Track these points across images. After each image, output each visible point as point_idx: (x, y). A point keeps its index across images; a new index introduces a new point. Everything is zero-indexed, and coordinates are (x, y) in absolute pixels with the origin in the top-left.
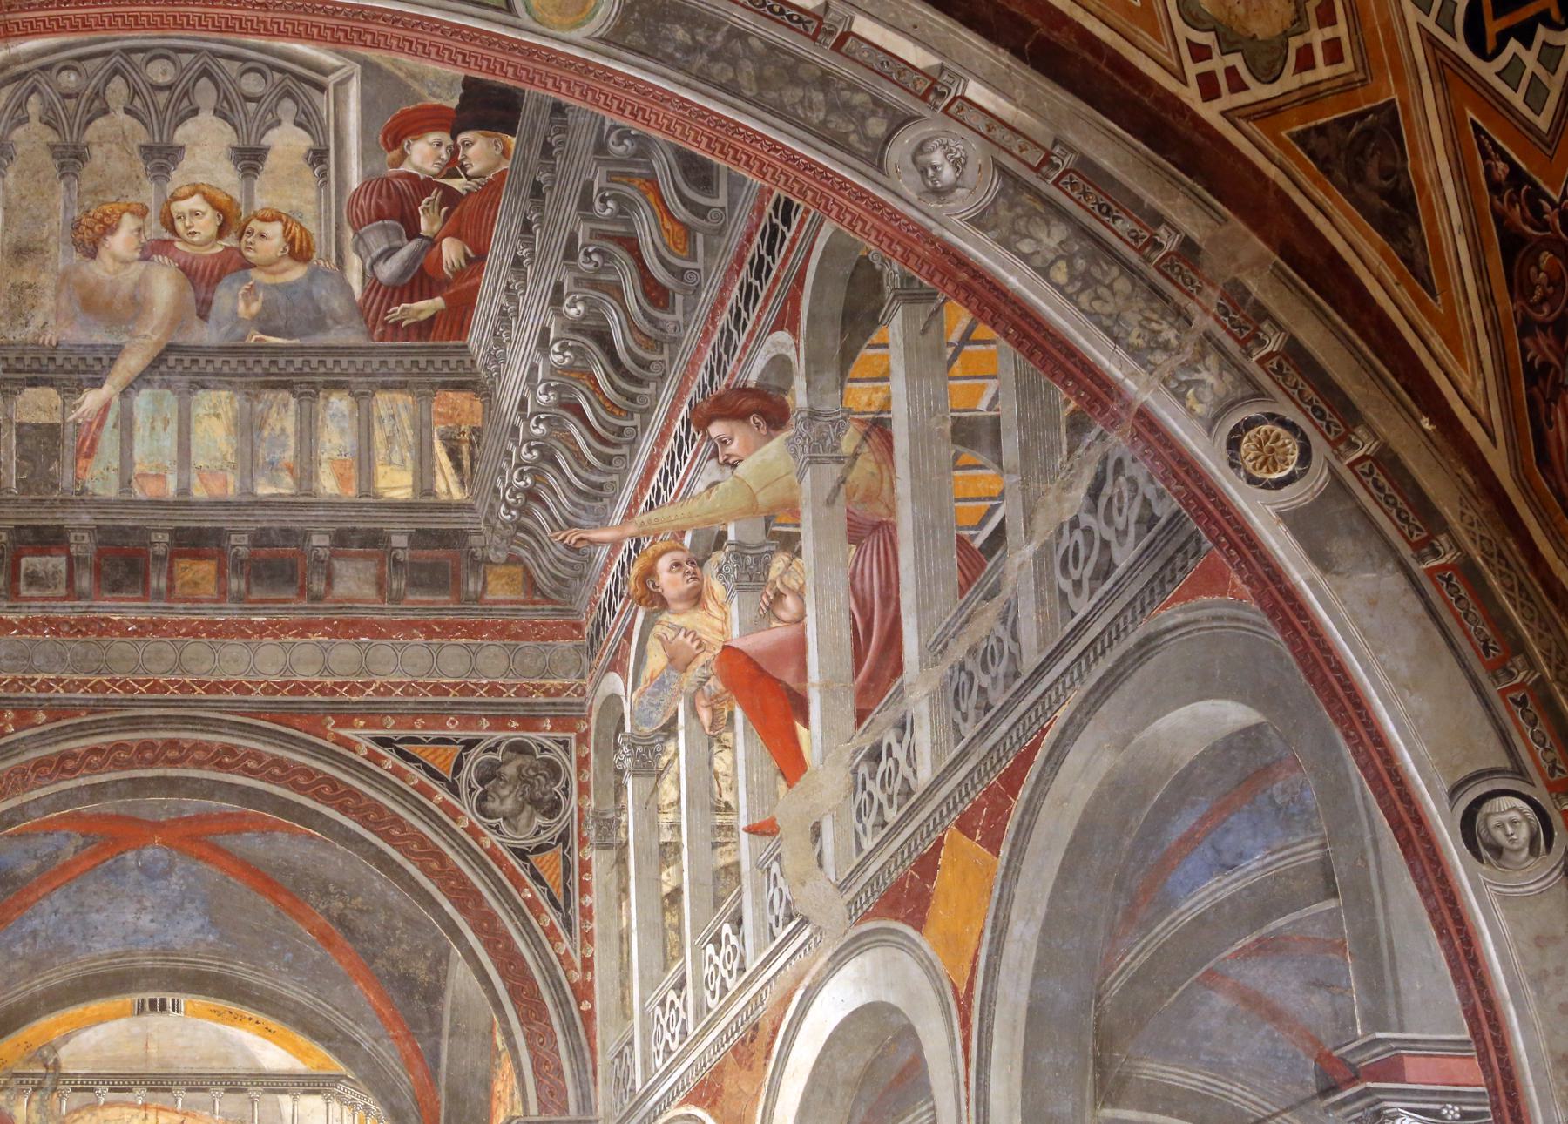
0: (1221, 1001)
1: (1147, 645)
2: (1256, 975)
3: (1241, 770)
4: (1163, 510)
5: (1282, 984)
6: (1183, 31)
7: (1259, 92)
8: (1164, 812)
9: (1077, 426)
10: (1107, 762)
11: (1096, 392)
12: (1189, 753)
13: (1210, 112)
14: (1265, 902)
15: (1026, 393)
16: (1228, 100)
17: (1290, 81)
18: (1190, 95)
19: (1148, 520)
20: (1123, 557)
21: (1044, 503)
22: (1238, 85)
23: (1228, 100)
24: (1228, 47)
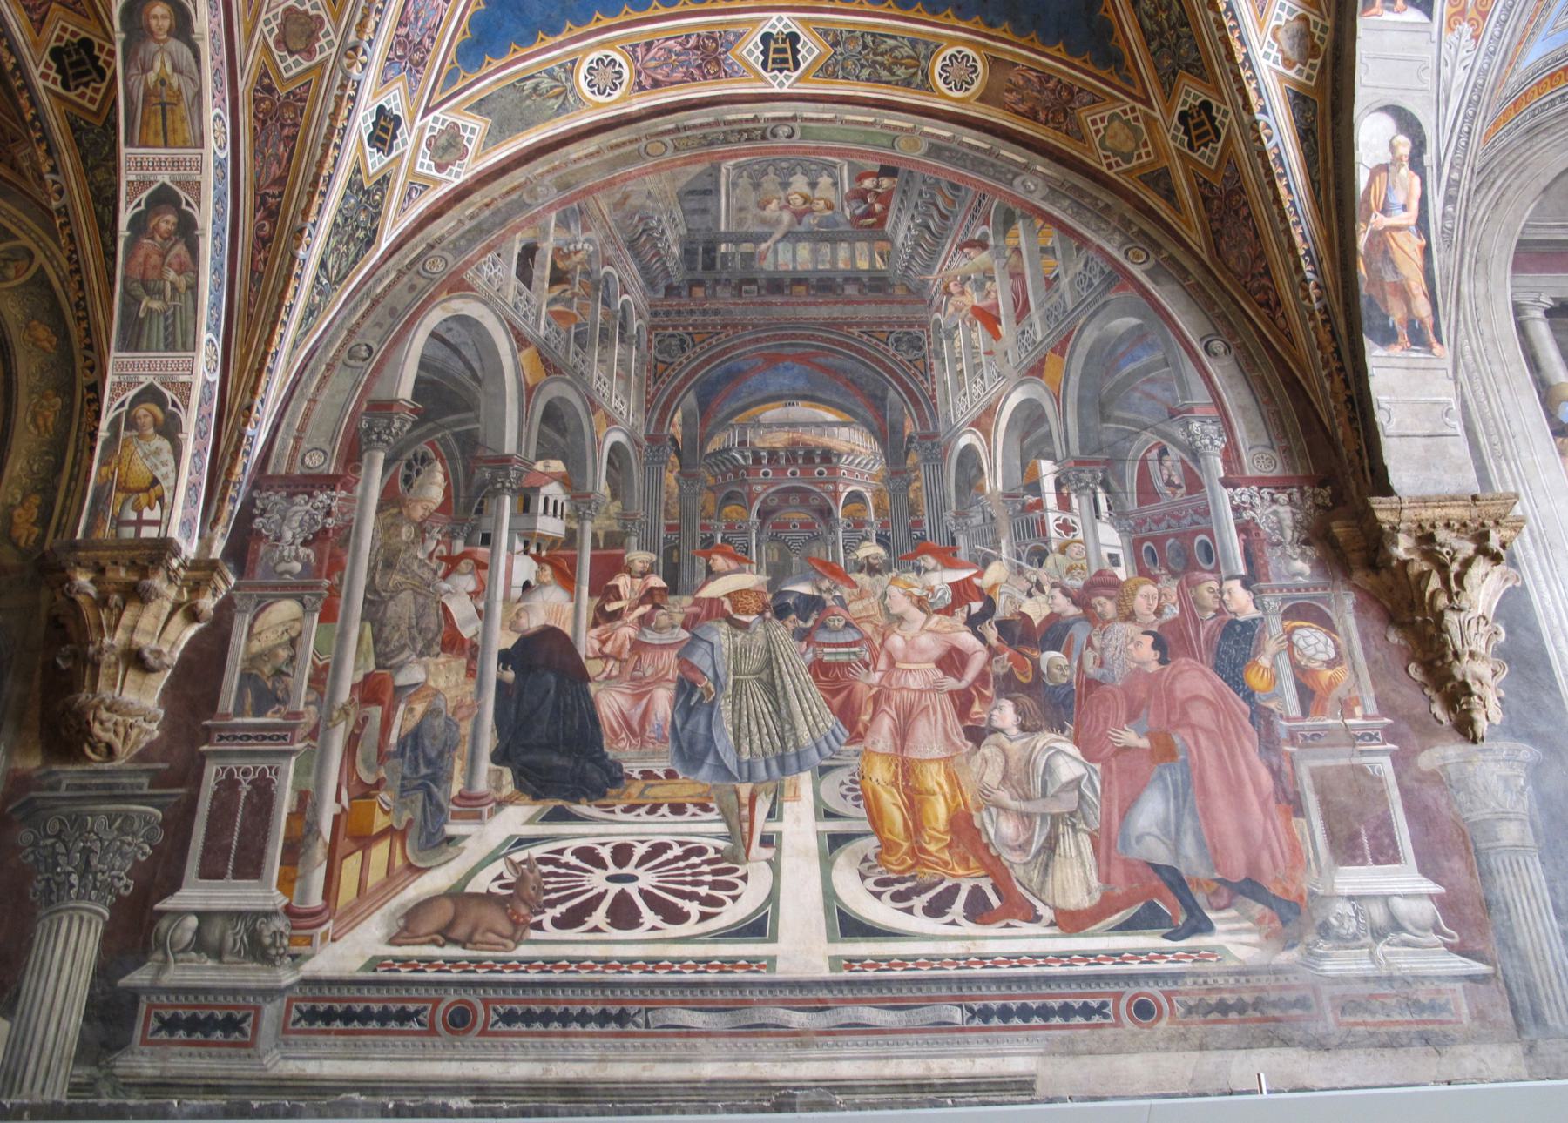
0: (1137, 395)
1: (1105, 304)
2: (1147, 388)
3: (1138, 337)
4: (1107, 270)
5: (1157, 391)
6: (1101, 152)
7: (1125, 166)
8: (1115, 347)
9: (1079, 249)
10: (1096, 334)
11: (1084, 242)
12: (1121, 331)
13: (1111, 173)
14: (1147, 369)
15: (1061, 241)
16: (1116, 169)
17: (1135, 163)
18: (1104, 169)
19: (1102, 272)
20: (1096, 282)
21: (1070, 270)
22: (1118, 164)
23: (1116, 169)
24: (1115, 155)
